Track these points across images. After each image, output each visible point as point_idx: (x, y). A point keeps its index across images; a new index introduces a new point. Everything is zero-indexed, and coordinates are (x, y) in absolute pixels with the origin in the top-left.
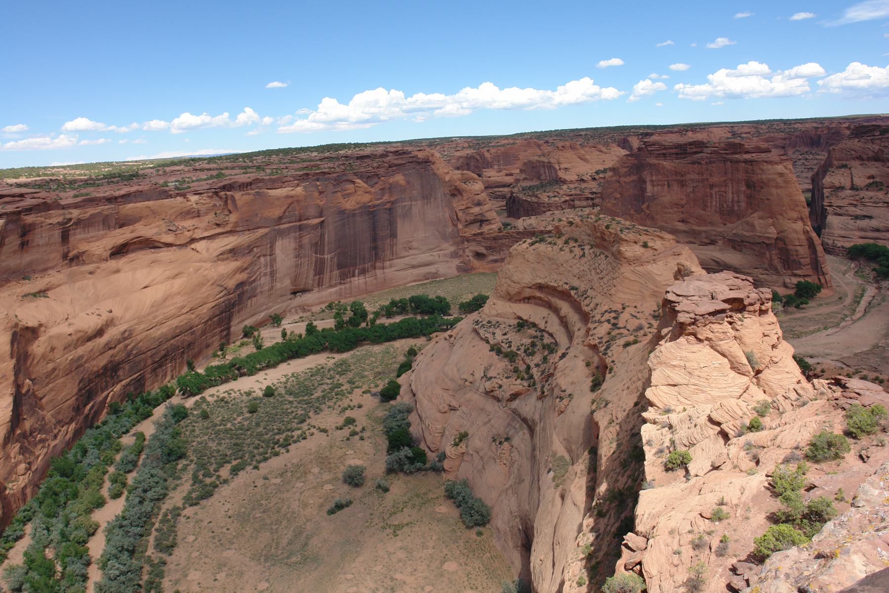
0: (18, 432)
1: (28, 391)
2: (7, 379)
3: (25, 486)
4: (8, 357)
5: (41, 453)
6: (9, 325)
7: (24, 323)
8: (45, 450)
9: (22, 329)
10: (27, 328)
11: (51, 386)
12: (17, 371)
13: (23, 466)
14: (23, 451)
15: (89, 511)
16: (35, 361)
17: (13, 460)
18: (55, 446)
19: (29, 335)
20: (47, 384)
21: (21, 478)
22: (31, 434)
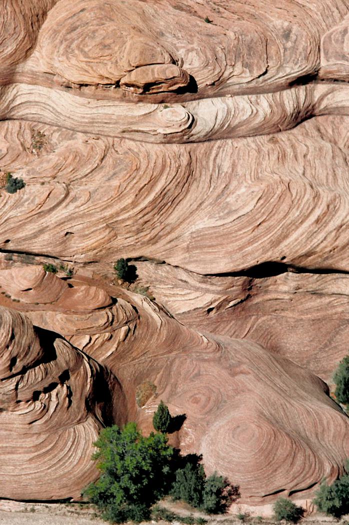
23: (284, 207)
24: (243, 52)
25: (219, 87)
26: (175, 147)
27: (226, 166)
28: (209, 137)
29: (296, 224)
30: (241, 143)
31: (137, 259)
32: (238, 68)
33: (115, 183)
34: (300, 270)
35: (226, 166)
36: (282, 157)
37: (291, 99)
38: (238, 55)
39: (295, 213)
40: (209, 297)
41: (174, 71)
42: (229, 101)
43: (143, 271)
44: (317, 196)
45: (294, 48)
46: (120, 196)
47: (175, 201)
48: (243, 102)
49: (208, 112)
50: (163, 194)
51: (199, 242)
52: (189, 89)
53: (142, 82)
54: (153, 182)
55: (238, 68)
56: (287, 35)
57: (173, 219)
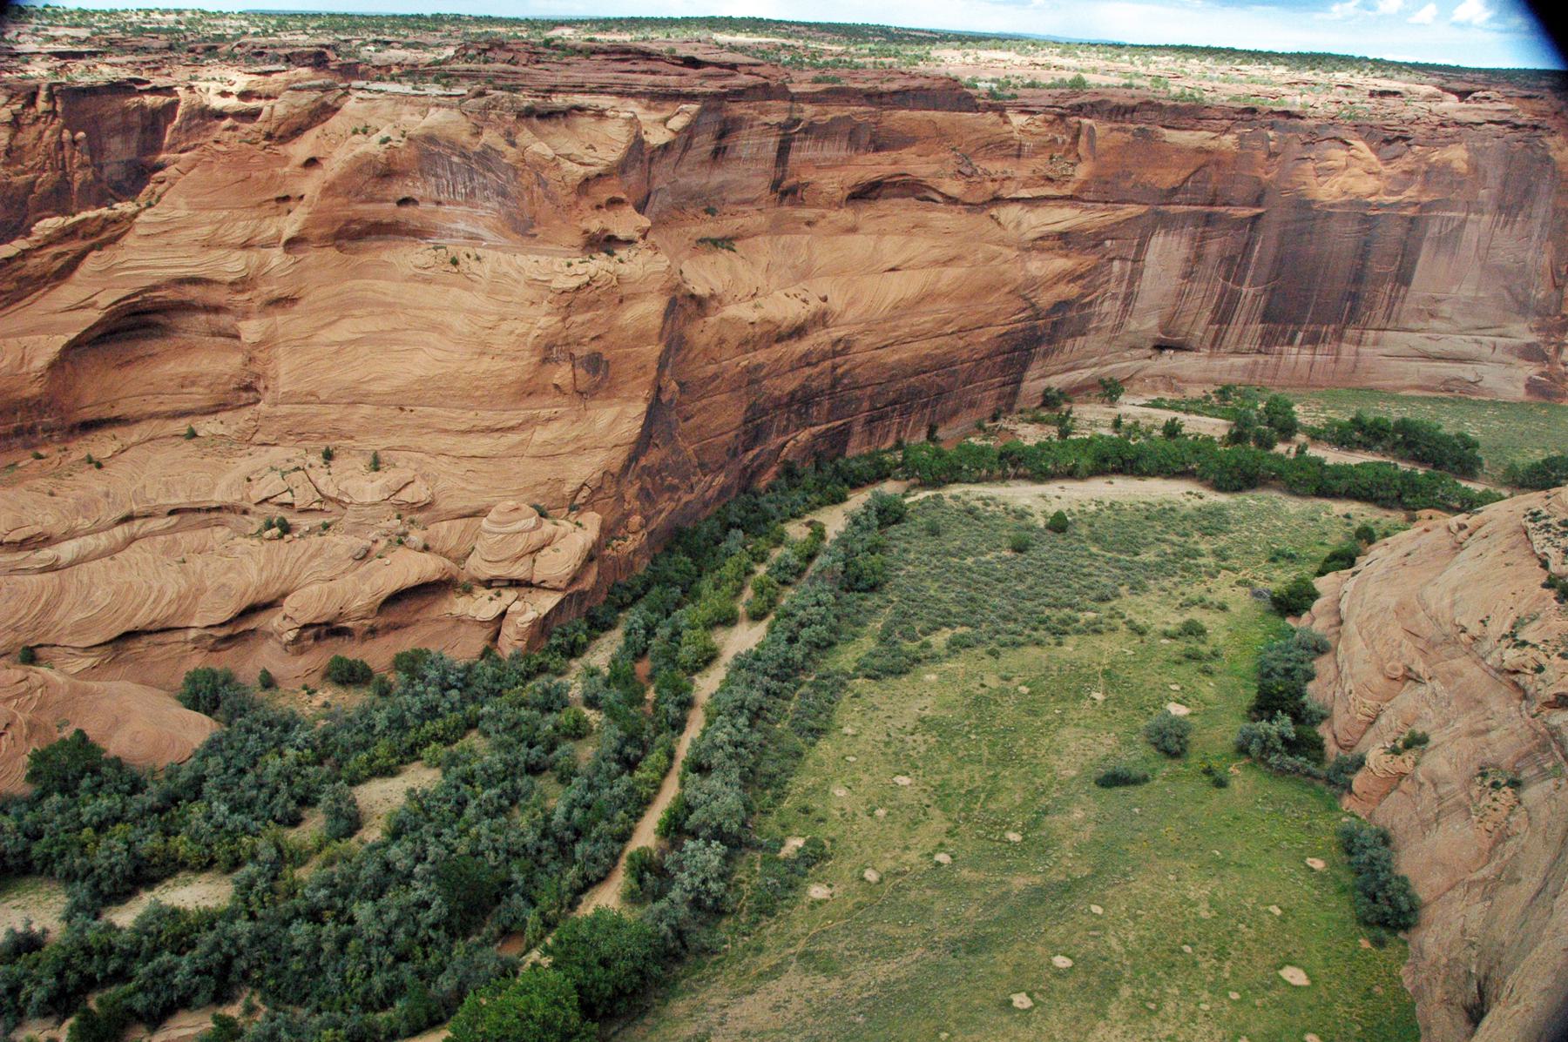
0: (643, 462)
1: (671, 400)
2: (645, 374)
3: (635, 552)
4: (655, 338)
5: (666, 506)
6: (669, 284)
7: (690, 287)
8: (673, 504)
9: (684, 296)
10: (693, 296)
11: (704, 402)
12: (662, 364)
13: (636, 519)
14: (645, 495)
15: (711, 625)
16: (692, 355)
17: (626, 506)
18: (686, 504)
19: (691, 308)
20: (699, 399)
21: (631, 537)
22: (659, 472)
23: (131, 596)
24: (84, 507)
25: (71, 534)
26: (49, 575)
27: (85, 579)
28: (70, 565)
29: (140, 607)
30: (93, 564)
31: (40, 646)
32: (80, 520)
33: (12, 603)
34: (150, 633)
35: (85, 579)
36: (121, 568)
37: (120, 532)
38: (78, 512)
39: (138, 600)
40: (91, 660)
41: (38, 529)
42: (80, 541)
43: (41, 652)
44: (150, 587)
45: (114, 503)
46: (17, 611)
47: (56, 607)
48: (89, 539)
49: (67, 550)
50: (47, 603)
51: (80, 629)
52: (47, 540)
53: (19, 538)
54: (39, 597)
55: (80, 520)
56: (107, 495)
57: (56, 618)
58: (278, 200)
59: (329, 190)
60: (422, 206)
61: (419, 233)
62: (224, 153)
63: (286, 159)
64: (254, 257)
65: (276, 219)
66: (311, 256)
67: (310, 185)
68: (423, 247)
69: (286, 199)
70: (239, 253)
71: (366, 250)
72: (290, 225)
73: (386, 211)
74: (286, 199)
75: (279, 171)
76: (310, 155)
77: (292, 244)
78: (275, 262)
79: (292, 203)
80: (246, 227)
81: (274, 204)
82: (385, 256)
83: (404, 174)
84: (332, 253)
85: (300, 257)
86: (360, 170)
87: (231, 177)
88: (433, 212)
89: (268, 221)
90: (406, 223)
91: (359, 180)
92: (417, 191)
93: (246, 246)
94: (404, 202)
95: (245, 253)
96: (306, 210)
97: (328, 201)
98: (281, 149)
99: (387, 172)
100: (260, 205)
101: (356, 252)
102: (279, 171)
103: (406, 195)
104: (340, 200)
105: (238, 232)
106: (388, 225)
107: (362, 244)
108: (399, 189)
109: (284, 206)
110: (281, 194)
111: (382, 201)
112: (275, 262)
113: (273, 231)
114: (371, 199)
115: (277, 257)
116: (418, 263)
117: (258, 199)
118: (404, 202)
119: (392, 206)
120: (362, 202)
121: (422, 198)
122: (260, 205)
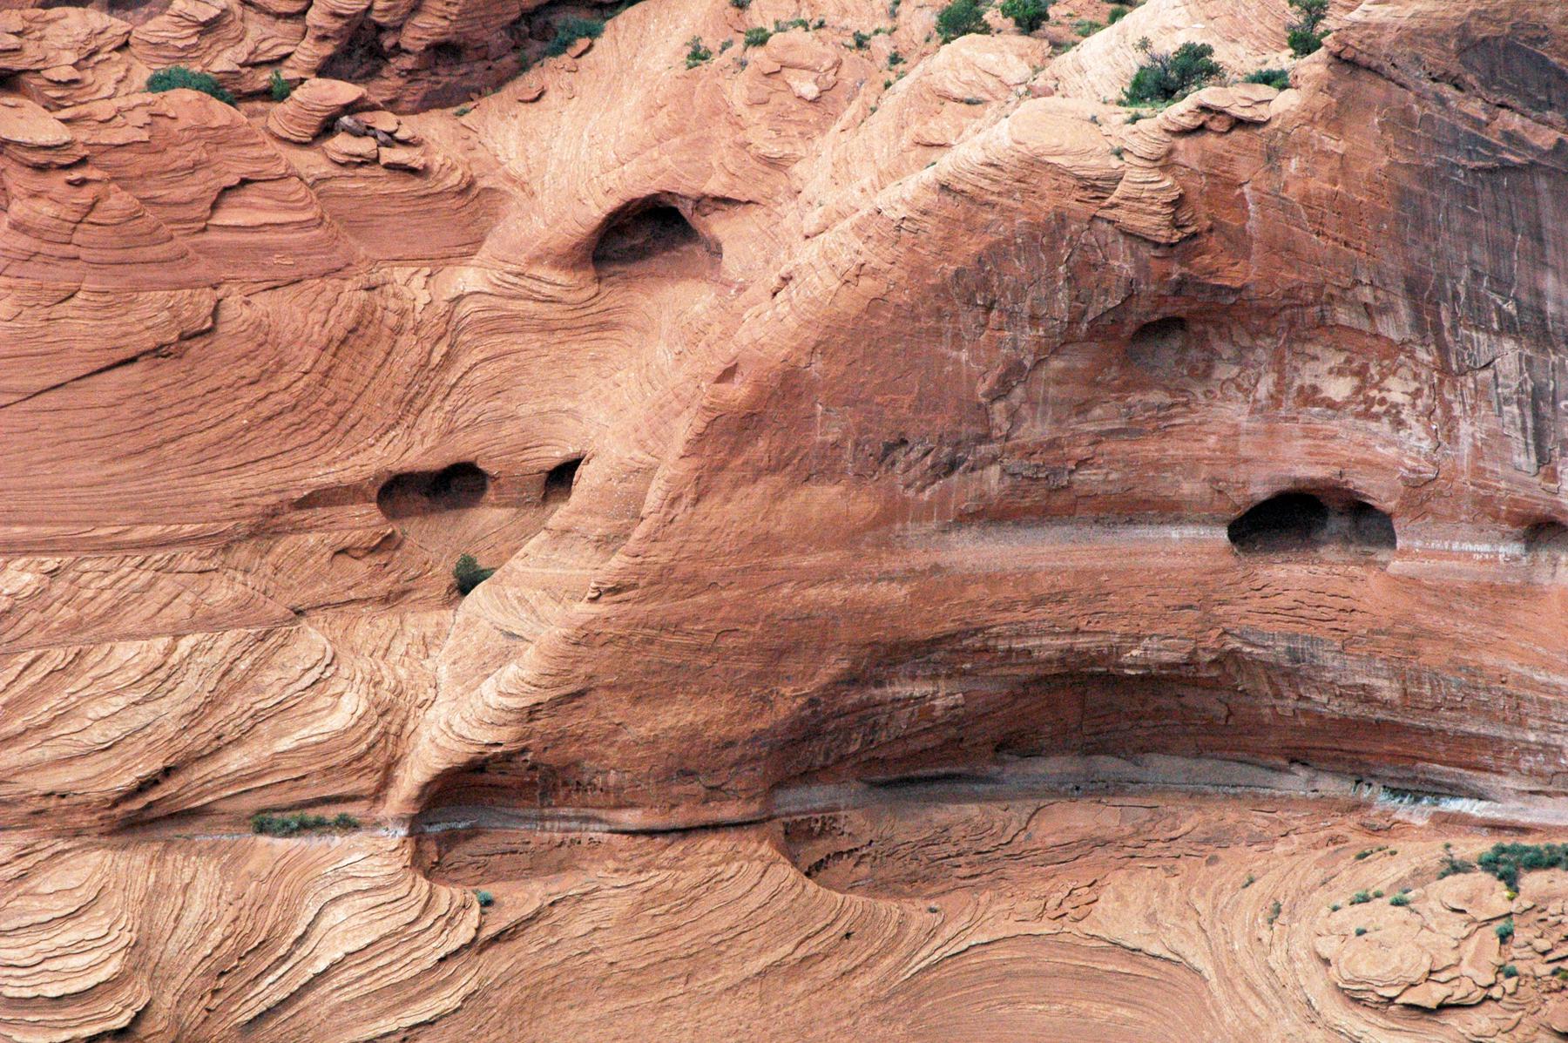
58: (399, 491)
59: (754, 425)
60: (1418, 553)
61: (1384, 750)
62: (43, 162)
63: (472, 204)
64: (200, 892)
65: (370, 628)
66: (598, 894)
67: (625, 398)
68: (1417, 851)
69: (457, 484)
70: (90, 867)
71: (990, 864)
72: (467, 670)
73: (1158, 580)
74: (457, 484)
75: (414, 289)
76: (636, 181)
77: (468, 805)
78: (343, 931)
79: (488, 517)
80: (159, 678)
81: (363, 520)
82: (1128, 909)
83: (1293, 319)
84: (747, 878)
85: (519, 898)
86: (975, 290)
87: (84, 328)
88: (1496, 595)
89: (313, 639)
90: (1293, 672)
91: (970, 360)
92: (1379, 445)
93: (147, 814)
94: (1287, 518)
95: (132, 866)
96: (585, 567)
97: (738, 510)
98: (436, 135)
99: (1163, 302)
100: (266, 527)
101: (919, 874)
102: (414, 289)
103: (1297, 462)
104: (824, 498)
105: (100, 718)
106: (1156, 680)
107: (960, 815)
108: (1247, 430)
109: (435, 540)
110: (419, 451)
111: (1131, 508)
112: (343, 931)
113: (341, 712)
114: (1045, 500)
115: (355, 896)
116: (1364, 965)
117: (258, 483)
118: (1287, 518)
119: (1195, 545)
120: (992, 516)
121: (1421, 495)
122: (266, 527)
